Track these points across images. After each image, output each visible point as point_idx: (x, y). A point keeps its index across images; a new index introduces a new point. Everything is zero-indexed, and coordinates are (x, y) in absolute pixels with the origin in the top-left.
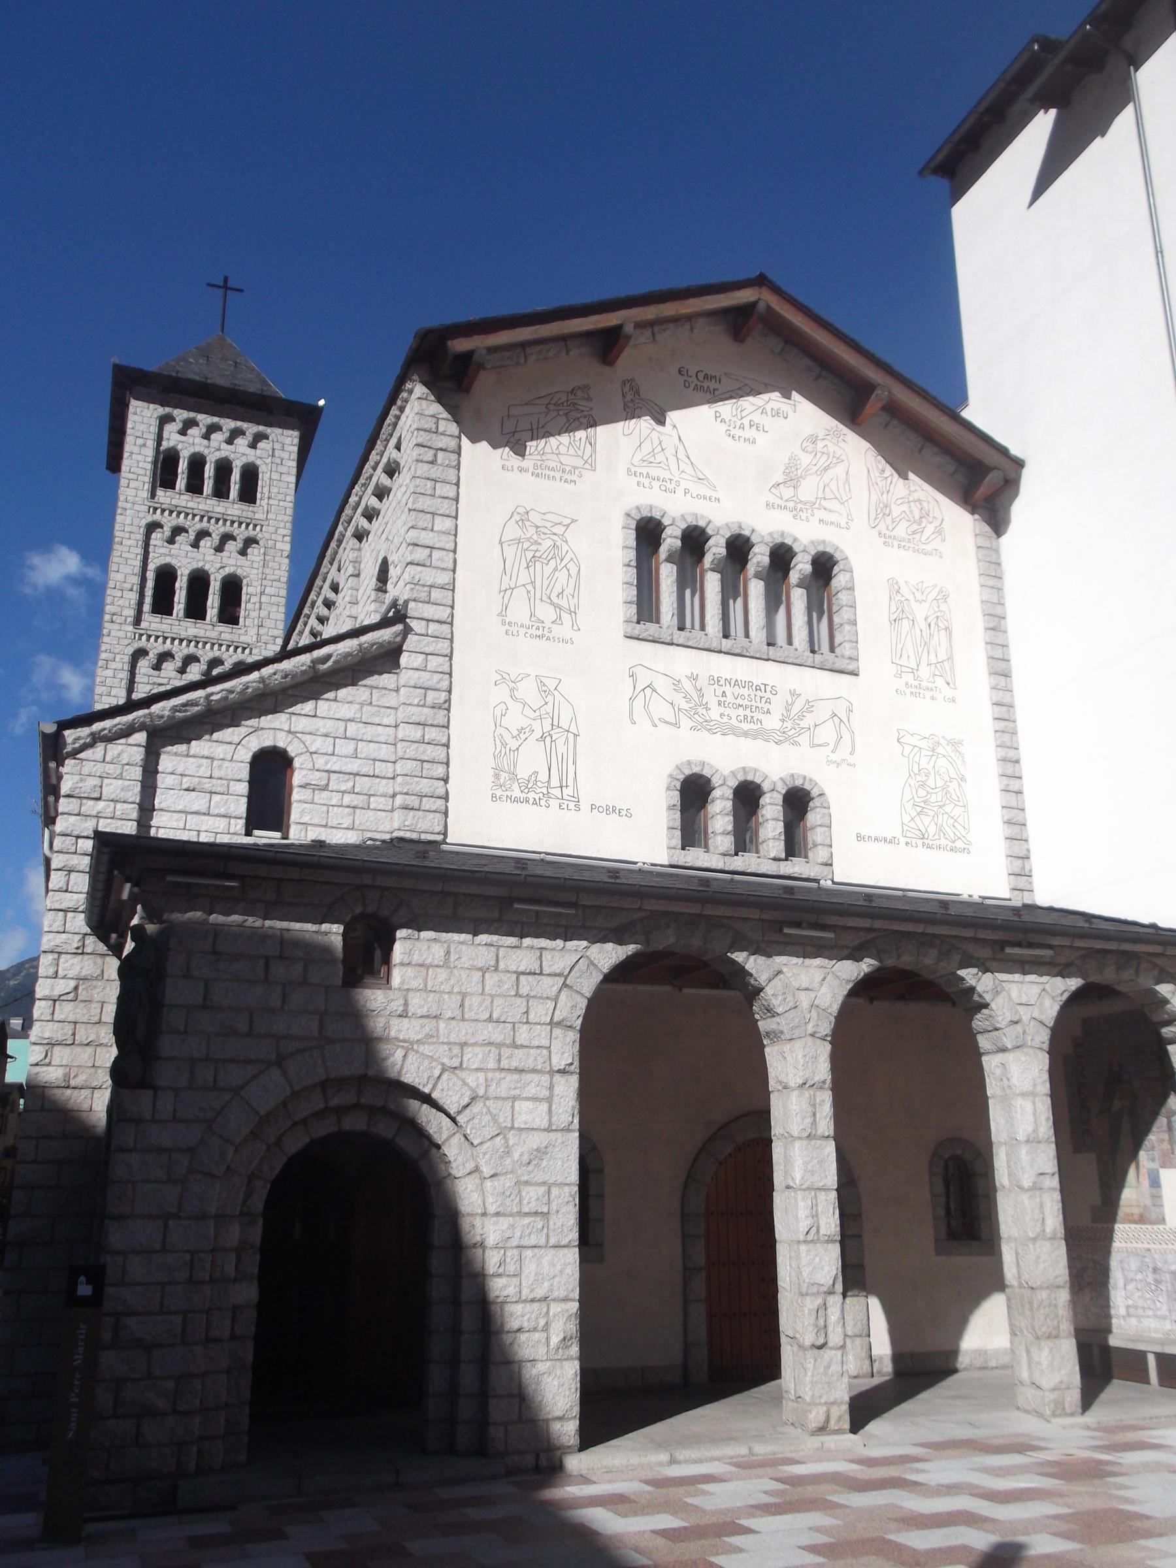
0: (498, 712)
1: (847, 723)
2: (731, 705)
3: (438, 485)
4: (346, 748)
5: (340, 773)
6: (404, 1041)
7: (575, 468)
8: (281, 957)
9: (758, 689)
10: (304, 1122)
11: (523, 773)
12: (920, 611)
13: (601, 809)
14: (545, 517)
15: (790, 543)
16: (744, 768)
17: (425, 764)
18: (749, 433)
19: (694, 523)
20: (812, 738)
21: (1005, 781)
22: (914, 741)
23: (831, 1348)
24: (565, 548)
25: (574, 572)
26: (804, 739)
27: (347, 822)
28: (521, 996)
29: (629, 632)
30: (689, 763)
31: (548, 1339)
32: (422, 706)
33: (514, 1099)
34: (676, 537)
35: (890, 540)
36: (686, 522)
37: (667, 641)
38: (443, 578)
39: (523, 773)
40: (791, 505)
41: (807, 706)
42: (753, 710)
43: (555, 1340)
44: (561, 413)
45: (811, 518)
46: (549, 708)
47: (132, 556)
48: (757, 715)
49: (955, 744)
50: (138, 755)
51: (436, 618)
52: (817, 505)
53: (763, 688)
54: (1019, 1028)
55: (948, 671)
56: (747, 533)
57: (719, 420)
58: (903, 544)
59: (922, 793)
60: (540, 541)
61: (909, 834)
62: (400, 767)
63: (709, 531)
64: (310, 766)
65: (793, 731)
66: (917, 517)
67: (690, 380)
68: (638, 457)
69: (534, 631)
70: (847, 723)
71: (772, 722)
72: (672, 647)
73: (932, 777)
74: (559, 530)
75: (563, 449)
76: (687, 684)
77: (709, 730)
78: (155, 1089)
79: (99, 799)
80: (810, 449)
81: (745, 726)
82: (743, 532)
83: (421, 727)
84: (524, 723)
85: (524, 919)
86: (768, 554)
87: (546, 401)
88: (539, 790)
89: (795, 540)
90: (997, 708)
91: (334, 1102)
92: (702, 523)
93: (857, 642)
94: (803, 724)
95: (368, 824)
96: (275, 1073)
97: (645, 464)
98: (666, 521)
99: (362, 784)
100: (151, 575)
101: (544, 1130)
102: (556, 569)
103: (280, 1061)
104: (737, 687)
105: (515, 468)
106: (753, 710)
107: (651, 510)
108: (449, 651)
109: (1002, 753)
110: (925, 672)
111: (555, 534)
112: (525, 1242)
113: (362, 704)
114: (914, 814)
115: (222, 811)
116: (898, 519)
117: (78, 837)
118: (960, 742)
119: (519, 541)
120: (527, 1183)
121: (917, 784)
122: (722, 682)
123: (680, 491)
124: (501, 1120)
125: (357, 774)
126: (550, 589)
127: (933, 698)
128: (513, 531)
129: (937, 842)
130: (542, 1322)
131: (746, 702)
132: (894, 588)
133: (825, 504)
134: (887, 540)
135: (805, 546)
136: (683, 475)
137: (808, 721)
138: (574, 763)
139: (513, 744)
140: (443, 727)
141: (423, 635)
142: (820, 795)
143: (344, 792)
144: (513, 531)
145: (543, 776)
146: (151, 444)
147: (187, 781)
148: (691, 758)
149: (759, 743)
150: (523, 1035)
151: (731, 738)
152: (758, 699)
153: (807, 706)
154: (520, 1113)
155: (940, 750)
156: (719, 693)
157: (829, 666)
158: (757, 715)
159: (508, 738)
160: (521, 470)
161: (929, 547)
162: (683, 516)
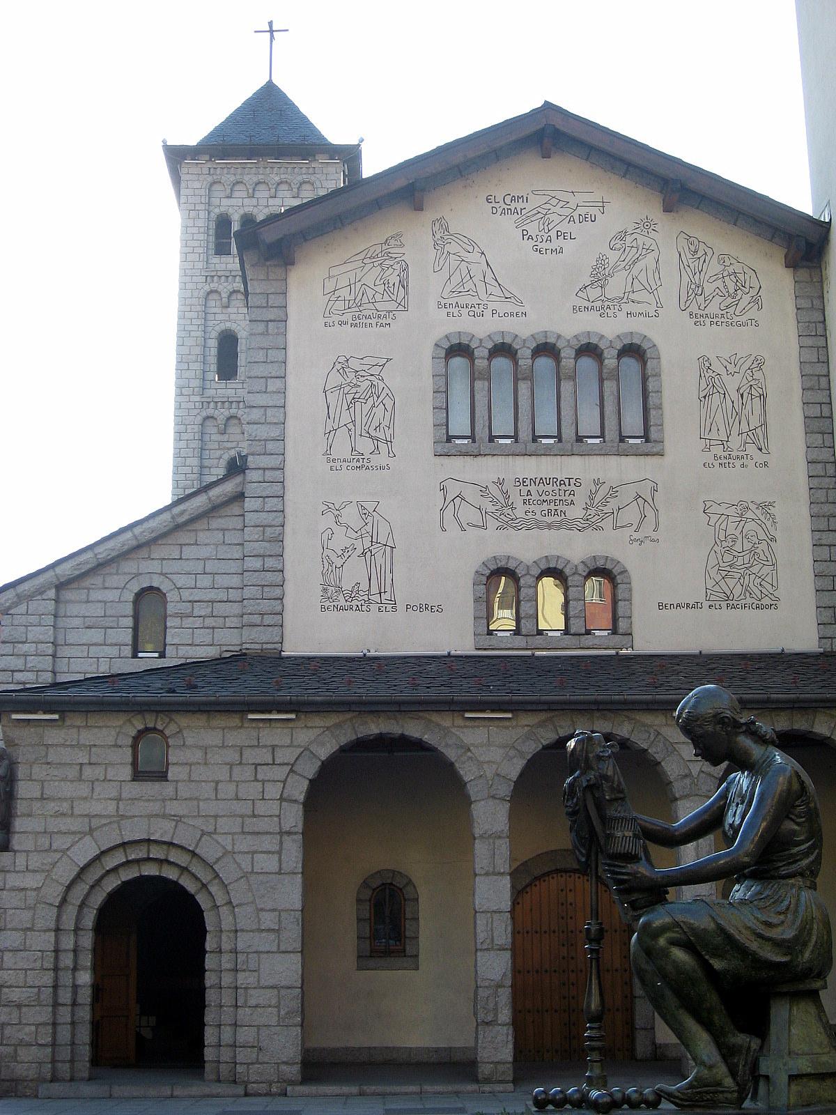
0: (325, 537)
1: (651, 502)
3: (270, 351)
4: (205, 581)
5: (199, 601)
6: (174, 816)
7: (389, 312)
8: (90, 764)
10: (115, 870)
11: (347, 585)
12: (732, 384)
13: (415, 608)
14: (362, 362)
17: (265, 587)
18: (555, 244)
21: (817, 535)
22: (721, 510)
23: (500, 1025)
24: (381, 385)
25: (389, 409)
26: (608, 523)
27: (208, 640)
28: (258, 781)
29: (440, 450)
31: (279, 1011)
32: (261, 541)
33: (254, 852)
34: (483, 358)
35: (702, 319)
38: (275, 432)
39: (347, 585)
40: (599, 304)
41: (611, 492)
43: (282, 1012)
44: (376, 264)
45: (618, 313)
46: (369, 528)
47: (195, 328)
48: (559, 508)
49: (765, 507)
50: (51, 606)
51: (270, 467)
52: (625, 300)
54: (688, 781)
55: (761, 440)
57: (526, 237)
58: (715, 320)
59: (728, 558)
60: (359, 383)
61: (713, 598)
62: (248, 592)
63: (515, 346)
64: (178, 599)
65: (597, 517)
66: (731, 291)
67: (497, 205)
68: (448, 289)
69: (355, 464)
70: (651, 502)
71: (576, 512)
72: (479, 458)
73: (739, 542)
74: (375, 370)
75: (378, 297)
76: (494, 490)
78: (15, 851)
79: (24, 642)
80: (618, 246)
81: (549, 519)
83: (261, 558)
84: (348, 543)
85: (261, 725)
87: (362, 256)
88: (362, 598)
90: (812, 466)
91: (133, 857)
95: (223, 640)
96: (88, 838)
97: (454, 295)
98: (473, 345)
99: (221, 609)
100: (213, 343)
101: (276, 873)
102: (373, 406)
103: (91, 831)
105: (336, 323)
108: (282, 492)
109: (816, 509)
110: (735, 442)
111: (372, 375)
112: (261, 949)
113: (217, 545)
114: (718, 578)
115: (114, 641)
116: (711, 297)
117: (13, 671)
118: (771, 504)
119: (340, 387)
120: (262, 910)
121: (723, 551)
122: (528, 482)
123: (488, 313)
124: (243, 866)
125: (212, 602)
126: (368, 424)
127: (743, 466)
128: (336, 378)
129: (743, 602)
130: (274, 1002)
131: (550, 497)
132: (705, 364)
133: (632, 296)
134: (698, 319)
136: (492, 298)
137: (613, 504)
138: (391, 572)
139: (339, 562)
140: (279, 555)
141: (260, 482)
143: (204, 617)
144: (336, 378)
145: (364, 586)
146: (203, 214)
147: (89, 622)
150: (261, 808)
152: (562, 493)
154: (258, 862)
155: (749, 515)
156: (524, 493)
158: (559, 508)
159: (333, 558)
160: (341, 323)
161: (743, 319)
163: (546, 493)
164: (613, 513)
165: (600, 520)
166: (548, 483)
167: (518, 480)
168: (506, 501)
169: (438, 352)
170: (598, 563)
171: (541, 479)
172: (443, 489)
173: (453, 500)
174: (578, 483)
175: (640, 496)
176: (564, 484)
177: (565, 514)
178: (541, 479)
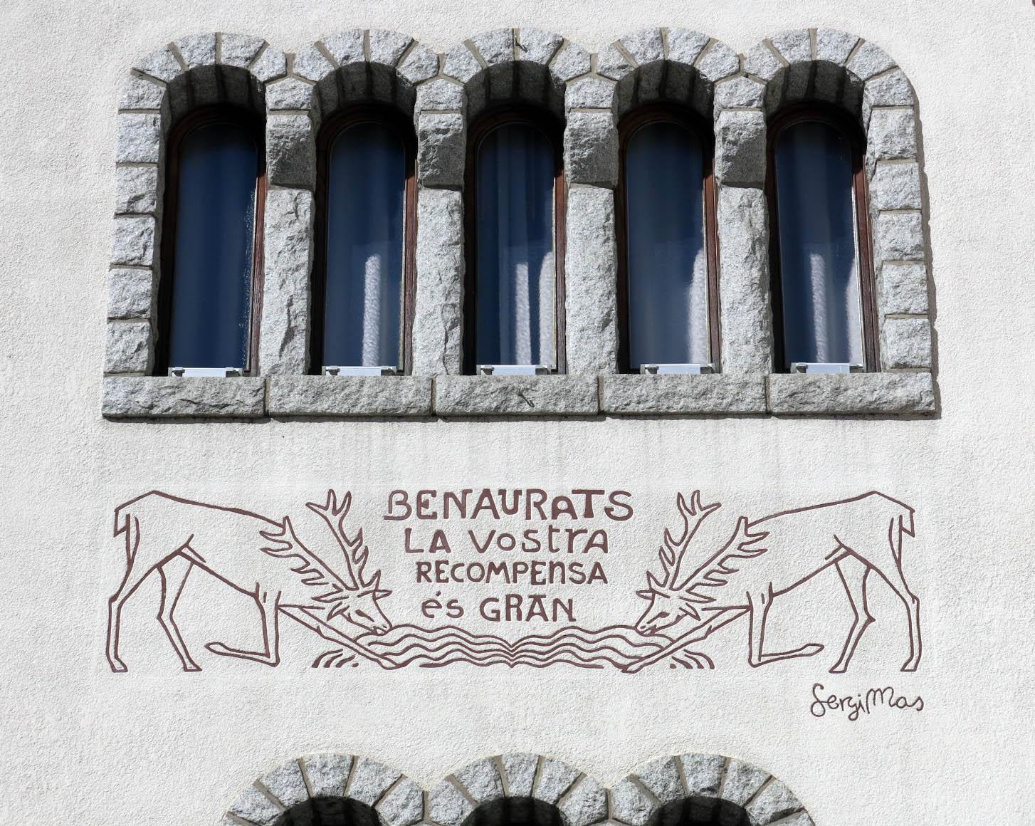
2: (460, 572)
9: (562, 506)
15: (687, 60)
16: (496, 762)
19: (358, 57)
20: (758, 635)
30: (301, 767)
36: (330, 59)
37: (243, 410)
41: (741, 537)
42: (544, 572)
53: (579, 503)
56: (536, 54)
63: (408, 72)
65: (687, 622)
76: (313, 532)
77: (377, 659)
82: (522, 56)
86: (608, 103)
89: (706, 46)
92: (381, 54)
93: (931, 313)
94: (722, 597)
98: (262, 70)
104: (486, 514)
106: (544, 572)
107: (216, 48)
122: (436, 505)
131: (518, 555)
135: (740, 59)
142: (786, 814)
148: (311, 754)
149: (561, 673)
151: (459, 672)
152: (560, 540)
153: (741, 537)
157: (821, 400)
158: (551, 591)
162: (319, 46)
163: (504, 540)
164: (749, 608)
165: (700, 633)
166: (510, 505)
167: (400, 497)
168: (355, 568)
169: (141, 91)
170: (690, 783)
171: (486, 493)
172: (127, 528)
173: (159, 566)
174: (619, 506)
175: (849, 552)
176: (570, 510)
177: (569, 612)
178: (486, 493)
